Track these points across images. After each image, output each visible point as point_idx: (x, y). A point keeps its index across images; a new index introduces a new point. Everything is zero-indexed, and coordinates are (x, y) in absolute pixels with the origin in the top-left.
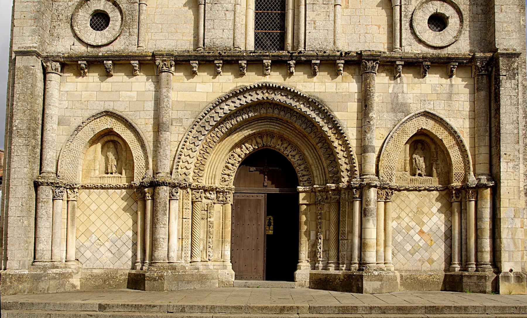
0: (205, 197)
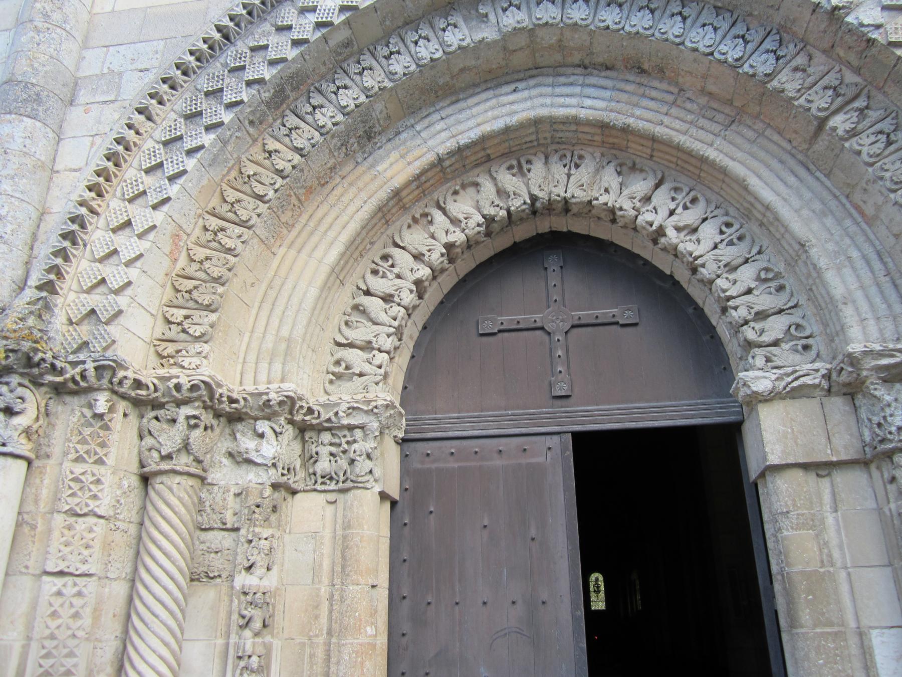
0: (231, 455)
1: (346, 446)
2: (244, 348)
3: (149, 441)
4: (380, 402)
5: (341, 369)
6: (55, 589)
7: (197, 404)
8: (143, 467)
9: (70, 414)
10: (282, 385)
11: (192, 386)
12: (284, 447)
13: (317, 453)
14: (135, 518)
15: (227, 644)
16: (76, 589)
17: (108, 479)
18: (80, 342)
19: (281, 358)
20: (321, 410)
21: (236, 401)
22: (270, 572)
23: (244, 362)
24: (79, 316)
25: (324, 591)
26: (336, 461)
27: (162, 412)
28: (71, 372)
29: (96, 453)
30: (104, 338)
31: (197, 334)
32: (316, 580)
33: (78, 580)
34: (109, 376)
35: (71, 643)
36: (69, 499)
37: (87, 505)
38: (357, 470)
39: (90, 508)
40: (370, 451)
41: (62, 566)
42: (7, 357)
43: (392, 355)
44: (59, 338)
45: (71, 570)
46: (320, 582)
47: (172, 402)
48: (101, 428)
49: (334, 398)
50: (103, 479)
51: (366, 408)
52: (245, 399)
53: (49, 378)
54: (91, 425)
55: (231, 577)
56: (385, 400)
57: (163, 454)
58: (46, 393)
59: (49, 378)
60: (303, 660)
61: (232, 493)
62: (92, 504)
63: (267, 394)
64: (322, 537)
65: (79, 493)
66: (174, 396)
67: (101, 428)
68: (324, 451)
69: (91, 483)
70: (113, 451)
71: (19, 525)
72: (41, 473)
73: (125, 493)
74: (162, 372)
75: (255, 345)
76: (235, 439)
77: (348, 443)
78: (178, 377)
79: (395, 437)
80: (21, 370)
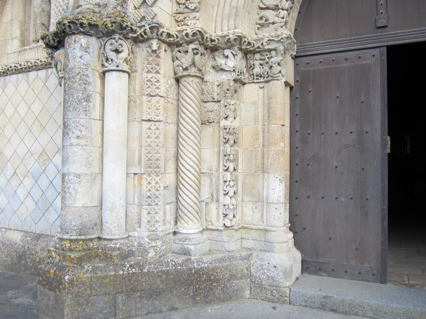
0: (214, 67)
1: (267, 60)
2: (215, 15)
3: (177, 62)
4: (284, 36)
5: (263, 22)
6: (147, 127)
7: (196, 42)
8: (176, 74)
9: (142, 51)
10: (235, 31)
11: (194, 34)
12: (238, 62)
13: (254, 65)
14: (175, 98)
15: (220, 150)
16: (156, 127)
17: (162, 80)
18: (141, 17)
19: (234, 18)
20: (254, 43)
21: (214, 41)
22: (236, 120)
23: (216, 22)
24: (139, 5)
25: (260, 128)
26: (263, 68)
27: (181, 48)
28: (140, 31)
29: (155, 69)
30: (151, 13)
31: (193, 8)
32: (256, 123)
33: (156, 123)
34: (156, 31)
35: (157, 148)
36: (147, 89)
37: (155, 92)
38: (274, 71)
39: (156, 93)
40: (279, 61)
41: (149, 118)
42: (112, 26)
43: (289, 12)
44: (132, 16)
45: (153, 119)
46: (258, 124)
47: (185, 43)
48: (156, 57)
49: (260, 36)
50: (160, 80)
51: (277, 40)
52: (218, 39)
53: (131, 35)
54: (152, 56)
55: (219, 122)
56: (287, 34)
57: (184, 68)
58: (130, 42)
59: (131, 35)
60: (252, 157)
61: (216, 85)
62: (157, 91)
63: (228, 36)
64: (258, 104)
65: (151, 87)
66: (186, 40)
67: (156, 57)
68: (257, 63)
69: (155, 82)
70: (162, 67)
71: (129, 101)
72: (134, 79)
73: (170, 86)
74: (179, 28)
75: (220, 12)
76: (215, 60)
77: (268, 58)
78: (186, 30)
79: (291, 55)
80: (119, 32)
